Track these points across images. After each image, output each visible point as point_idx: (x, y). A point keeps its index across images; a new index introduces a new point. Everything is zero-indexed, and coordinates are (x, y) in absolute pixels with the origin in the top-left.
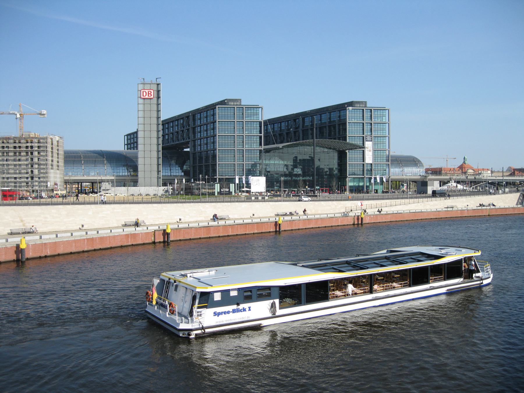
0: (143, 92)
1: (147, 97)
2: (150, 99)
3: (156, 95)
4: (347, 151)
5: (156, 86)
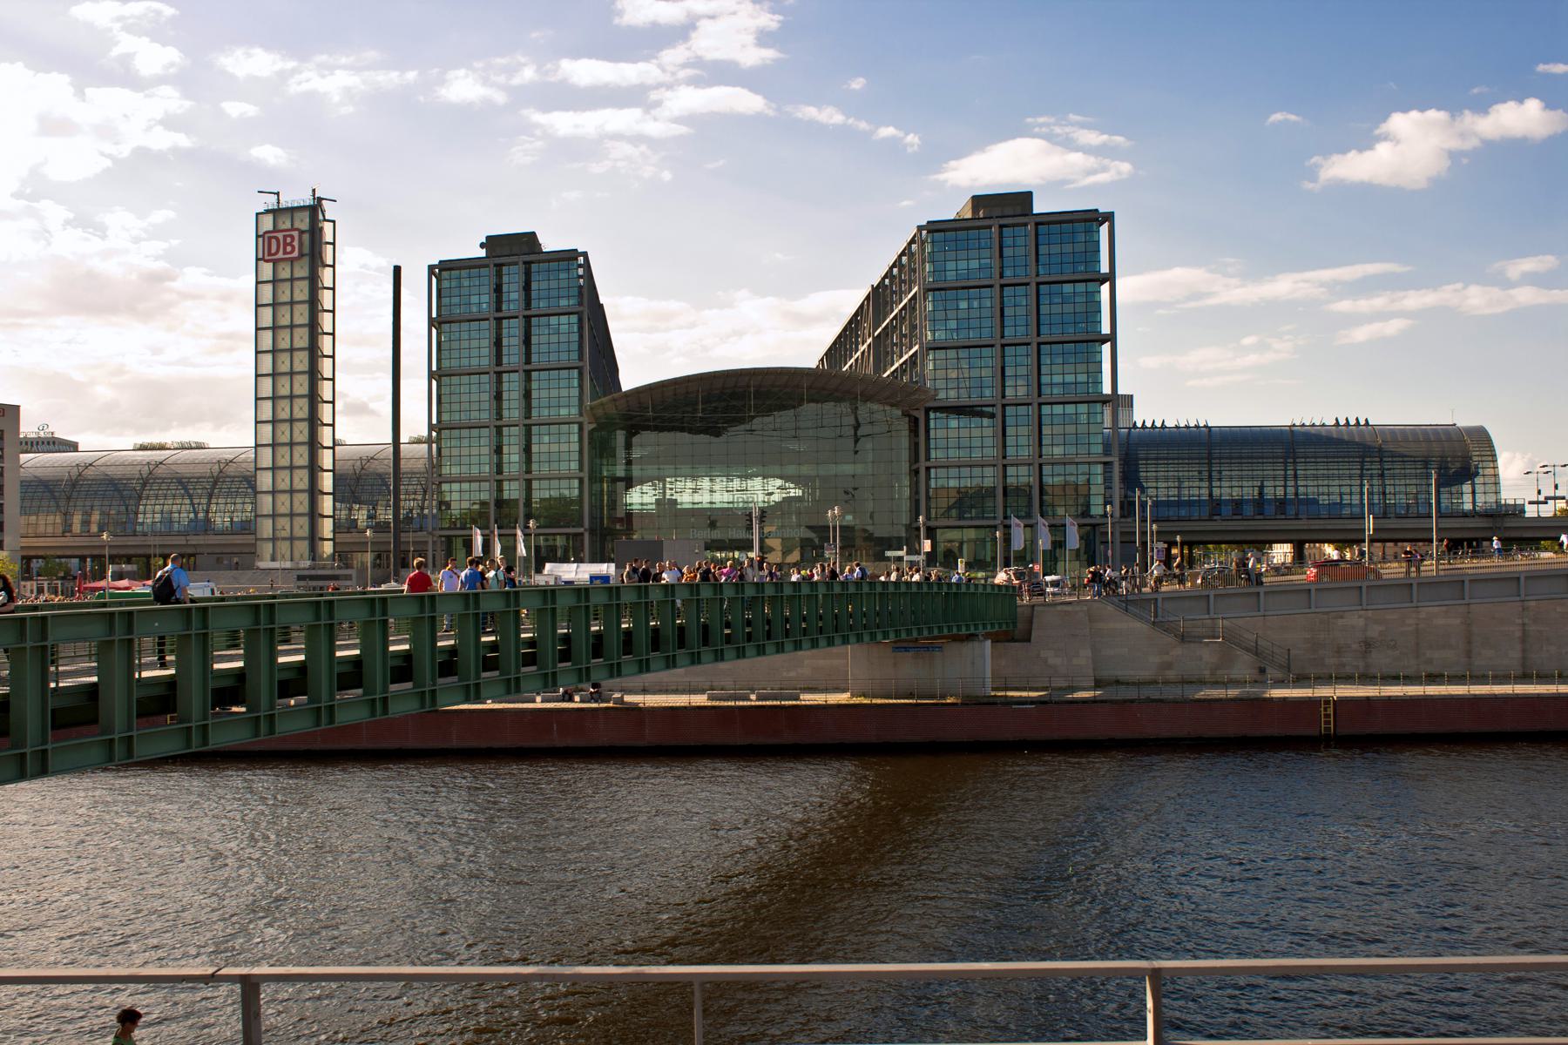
0: (270, 238)
1: (280, 255)
2: (292, 260)
3: (306, 250)
4: (921, 415)
5: (306, 215)
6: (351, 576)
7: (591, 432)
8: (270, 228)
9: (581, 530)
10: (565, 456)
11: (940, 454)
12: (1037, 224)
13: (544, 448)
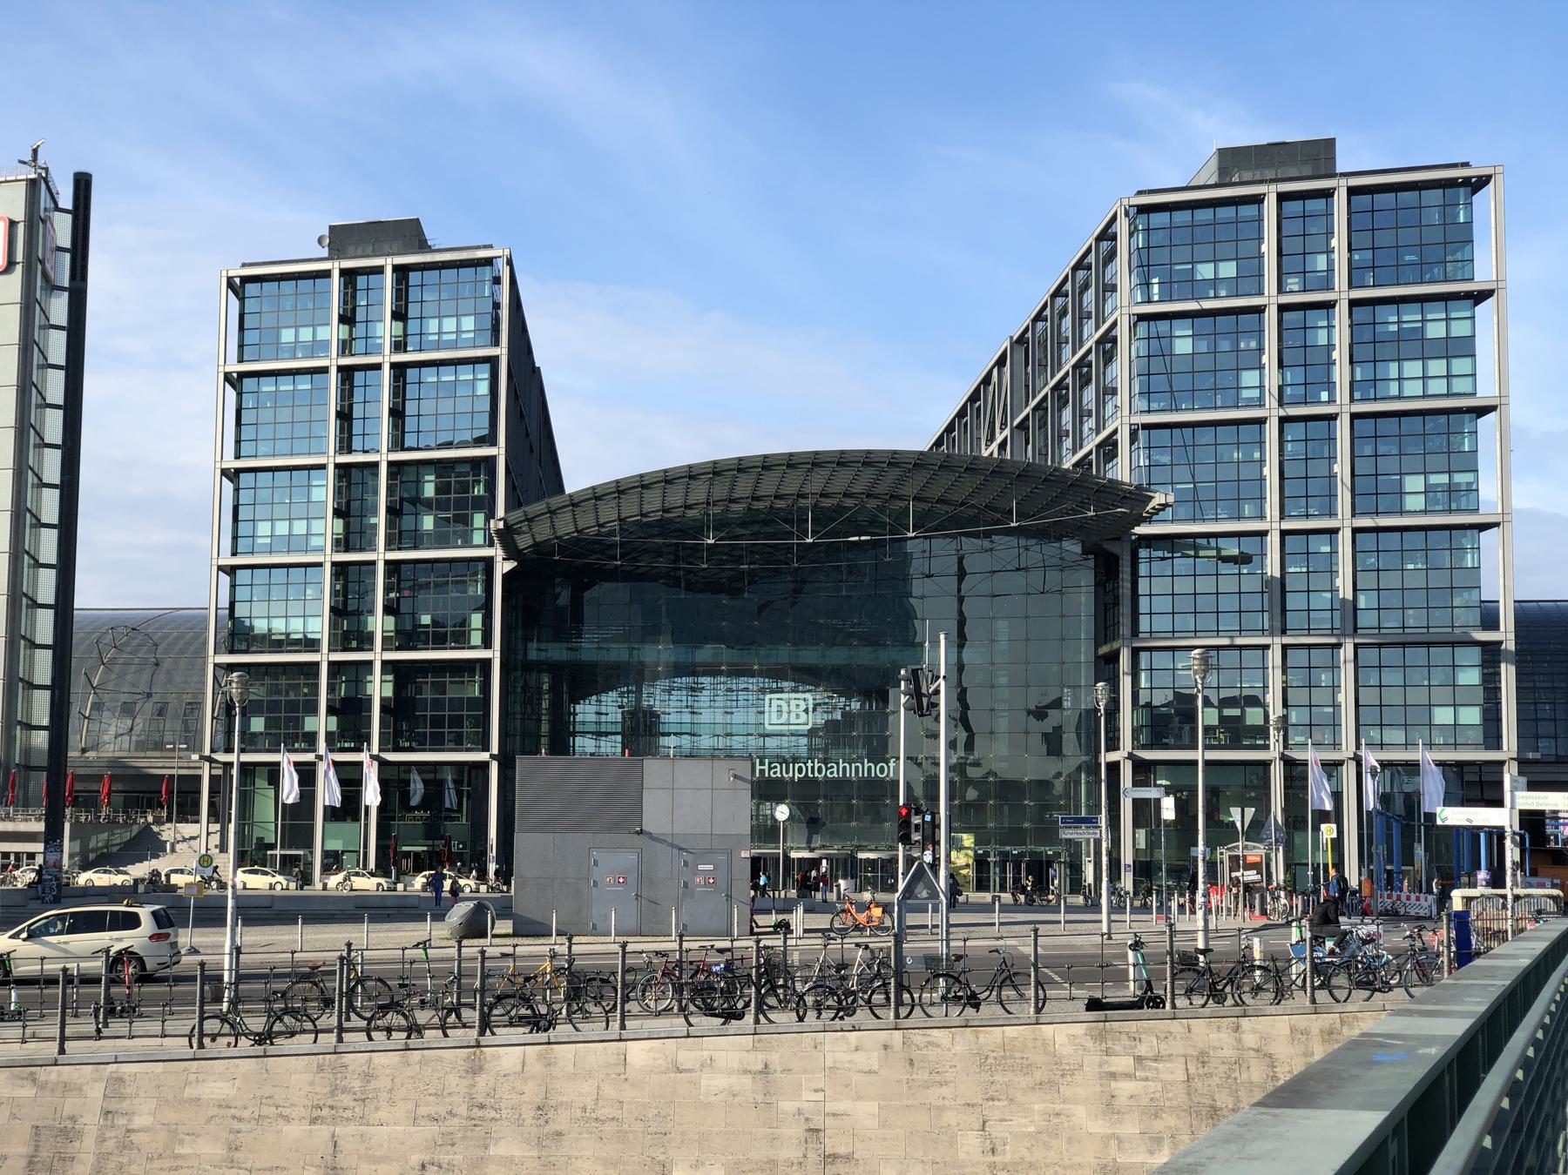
3: (19, 257)
7: (503, 575)
9: (484, 756)
11: (1162, 623)
12: (1352, 191)
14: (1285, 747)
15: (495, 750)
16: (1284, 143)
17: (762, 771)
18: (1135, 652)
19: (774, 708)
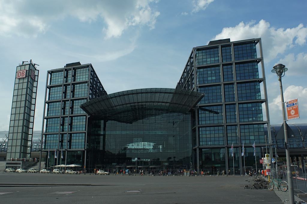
0: (19, 73)
1: (21, 77)
2: (23, 78)
3: (27, 75)
6: (20, 163)
8: (20, 70)
9: (84, 149)
10: (81, 126)
11: (204, 123)
13: (76, 124)
14: (227, 144)
15: (86, 149)
16: (221, 40)
17: (133, 152)
18: (199, 128)
19: (135, 140)
